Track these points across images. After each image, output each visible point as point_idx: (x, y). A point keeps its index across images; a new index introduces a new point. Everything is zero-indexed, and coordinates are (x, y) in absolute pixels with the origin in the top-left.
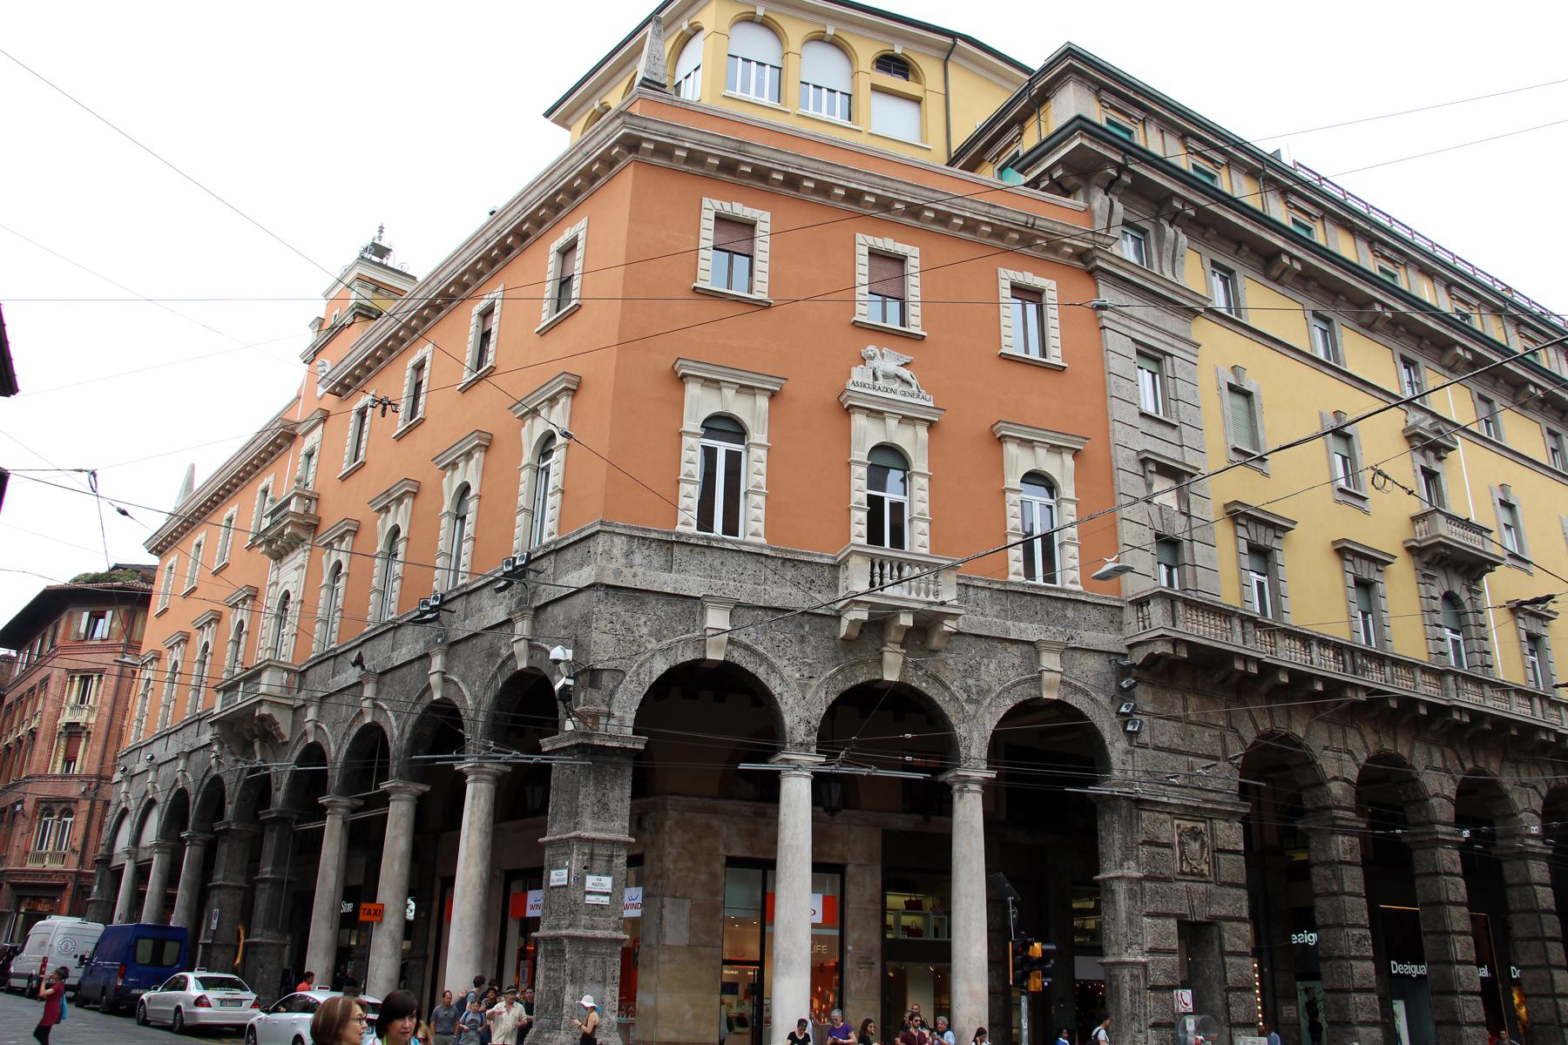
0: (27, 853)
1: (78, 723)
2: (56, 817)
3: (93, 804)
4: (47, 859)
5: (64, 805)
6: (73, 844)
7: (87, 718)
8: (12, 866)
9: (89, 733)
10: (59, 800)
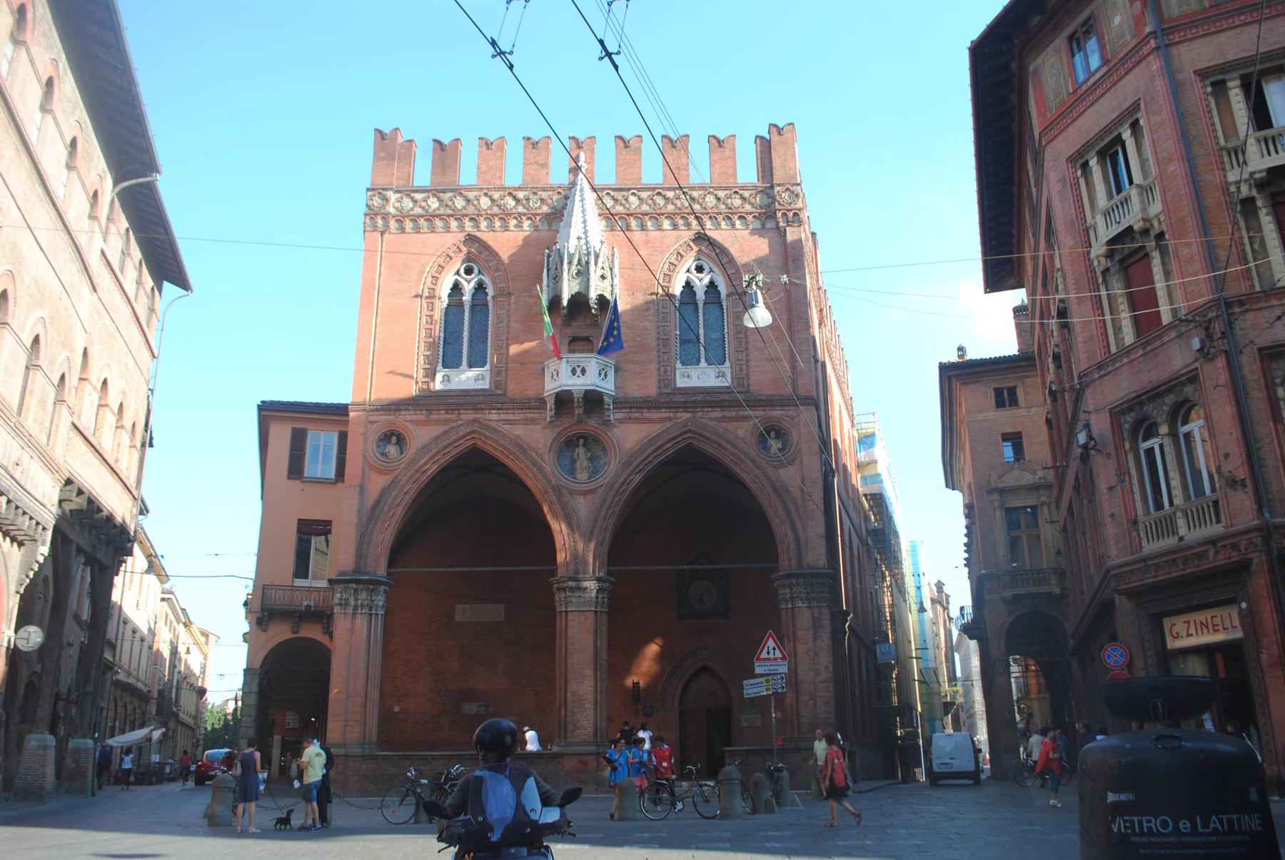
0: (1135, 522)
1: (1130, 228)
2: (1164, 429)
3: (1233, 368)
4: (1181, 522)
5: (1170, 400)
6: (1225, 469)
7: (1144, 210)
8: (1116, 555)
9: (1161, 236)
10: (1155, 394)
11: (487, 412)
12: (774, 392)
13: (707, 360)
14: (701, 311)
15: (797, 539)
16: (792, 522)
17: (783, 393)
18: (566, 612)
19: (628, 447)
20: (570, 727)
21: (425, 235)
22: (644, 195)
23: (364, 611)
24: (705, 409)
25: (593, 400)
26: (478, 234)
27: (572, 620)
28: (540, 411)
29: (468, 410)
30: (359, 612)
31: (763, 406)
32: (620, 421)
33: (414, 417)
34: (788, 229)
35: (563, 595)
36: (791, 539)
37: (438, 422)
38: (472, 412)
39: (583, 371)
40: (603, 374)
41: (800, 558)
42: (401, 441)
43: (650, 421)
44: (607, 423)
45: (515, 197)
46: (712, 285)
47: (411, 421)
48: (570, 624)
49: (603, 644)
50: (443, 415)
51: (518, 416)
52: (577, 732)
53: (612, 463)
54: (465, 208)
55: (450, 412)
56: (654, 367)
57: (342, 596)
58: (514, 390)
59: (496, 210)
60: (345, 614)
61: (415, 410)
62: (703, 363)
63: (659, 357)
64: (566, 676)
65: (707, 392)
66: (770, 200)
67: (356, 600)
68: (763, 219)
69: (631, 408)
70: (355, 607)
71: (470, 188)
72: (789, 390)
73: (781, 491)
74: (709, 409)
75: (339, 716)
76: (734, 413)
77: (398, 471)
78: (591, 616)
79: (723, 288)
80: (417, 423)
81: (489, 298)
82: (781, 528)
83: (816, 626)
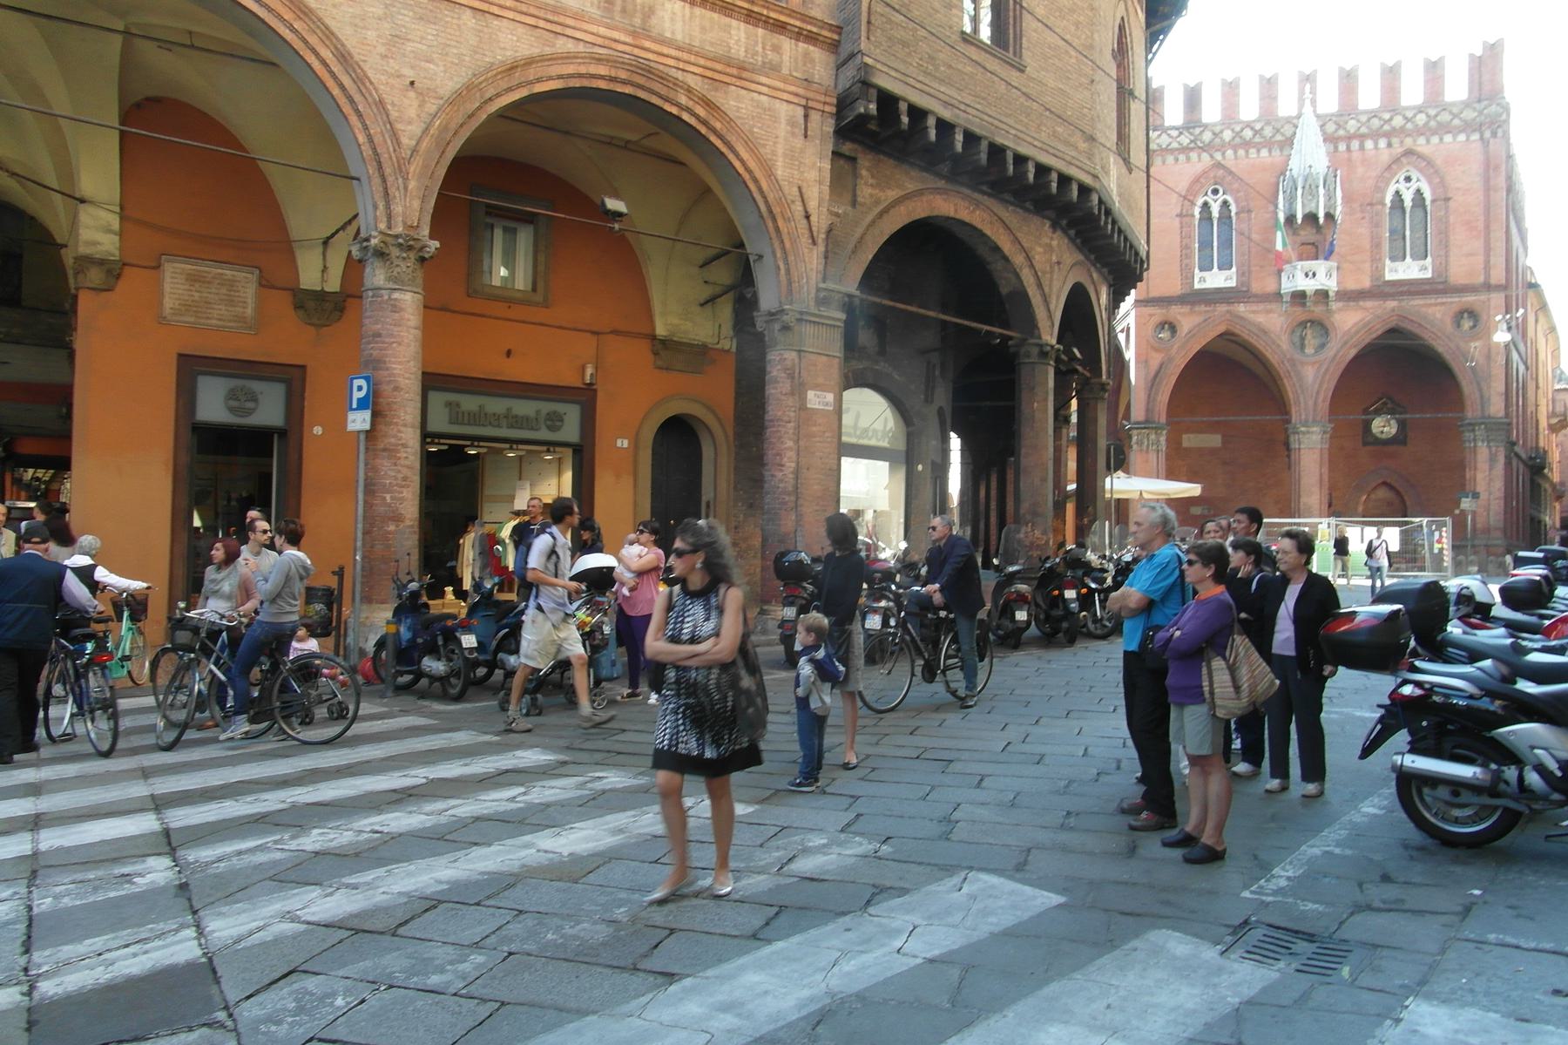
13: (1412, 256)
14: (1408, 215)
15: (1482, 397)
16: (1478, 384)
25: (1323, 295)
32: (1340, 310)
34: (1492, 141)
36: (1477, 395)
39: (1314, 275)
40: (1329, 275)
41: (1483, 410)
42: (1173, 328)
44: (1329, 311)
45: (1252, 129)
46: (1418, 192)
49: (1325, 470)
51: (1261, 307)
56: (1367, 266)
58: (1256, 287)
79: (1428, 195)
80: (1183, 314)
81: (1233, 214)
82: (1467, 387)
83: (1492, 459)
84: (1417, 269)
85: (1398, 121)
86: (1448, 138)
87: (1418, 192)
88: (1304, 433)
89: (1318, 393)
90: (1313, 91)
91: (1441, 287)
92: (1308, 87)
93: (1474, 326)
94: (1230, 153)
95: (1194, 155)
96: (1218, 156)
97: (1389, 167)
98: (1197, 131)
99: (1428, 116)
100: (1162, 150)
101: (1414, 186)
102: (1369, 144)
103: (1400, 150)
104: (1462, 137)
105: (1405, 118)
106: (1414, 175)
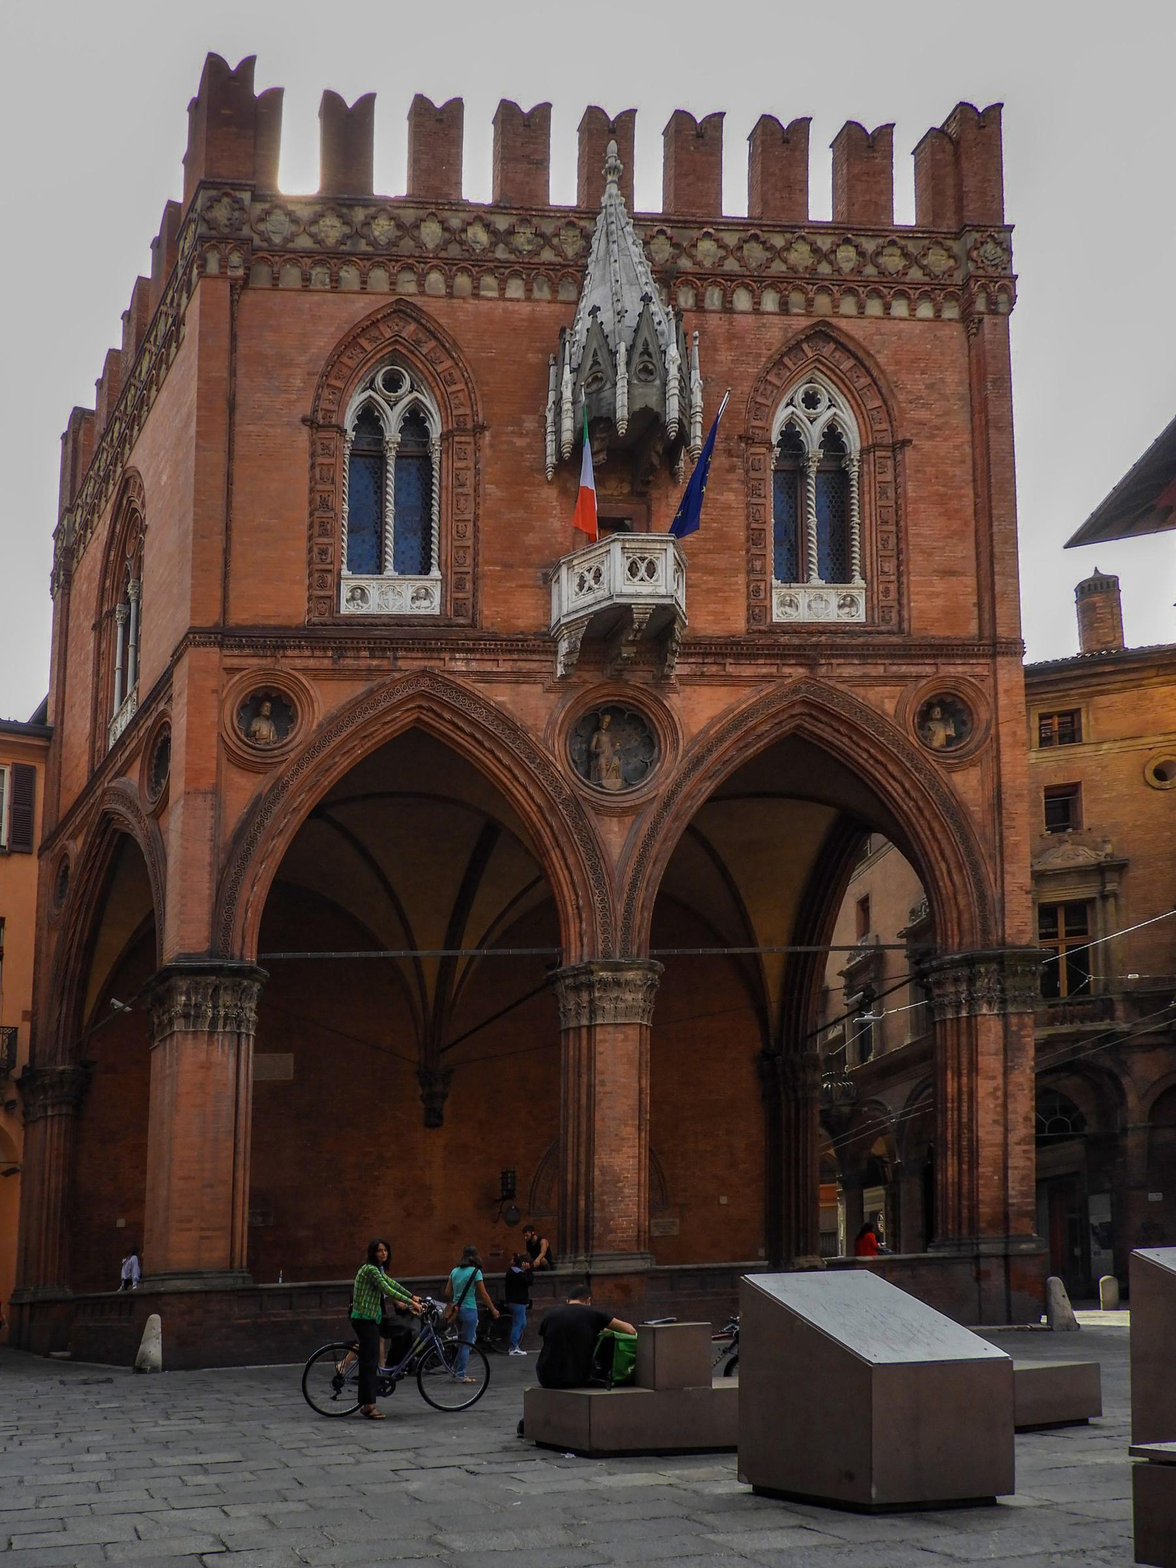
11: (447, 656)
12: (948, 633)
17: (963, 635)
18: (591, 1028)
19: (695, 731)
20: (598, 1228)
21: (316, 297)
22: (731, 239)
23: (227, 1029)
24: (834, 661)
26: (418, 301)
27: (602, 1041)
28: (543, 657)
29: (412, 650)
30: (220, 1029)
31: (935, 656)
32: (685, 680)
33: (311, 663)
34: (986, 316)
35: (585, 996)
37: (355, 675)
38: (420, 655)
41: (986, 932)
43: (734, 681)
45: (487, 226)
46: (832, 438)
47: (305, 670)
48: (599, 1049)
50: (366, 661)
52: (610, 1237)
53: (669, 756)
54: (393, 243)
55: (377, 654)
56: (741, 579)
57: (189, 999)
58: (491, 614)
59: (454, 251)
60: (195, 1033)
61: (313, 649)
62: (815, 580)
63: (748, 562)
64: (590, 1140)
65: (831, 632)
66: (951, 262)
67: (215, 1007)
68: (940, 299)
69: (705, 655)
70: (214, 1022)
71: (399, 203)
72: (973, 628)
73: (955, 810)
74: (842, 661)
75: (190, 1221)
76: (881, 669)
77: (284, 766)
78: (633, 1033)
79: (853, 441)
80: (316, 674)
84: (834, 601)
85: (800, 255)
86: (900, 308)
87: (832, 438)
88: (605, 985)
89: (633, 885)
90: (626, 154)
91: (894, 639)
92: (613, 146)
93: (959, 736)
94: (435, 278)
95: (349, 275)
96: (408, 285)
97: (779, 363)
98: (359, 214)
99: (861, 254)
100: (273, 250)
101: (824, 415)
102: (742, 300)
103: (804, 322)
104: (925, 310)
105: (815, 250)
106: (826, 389)
